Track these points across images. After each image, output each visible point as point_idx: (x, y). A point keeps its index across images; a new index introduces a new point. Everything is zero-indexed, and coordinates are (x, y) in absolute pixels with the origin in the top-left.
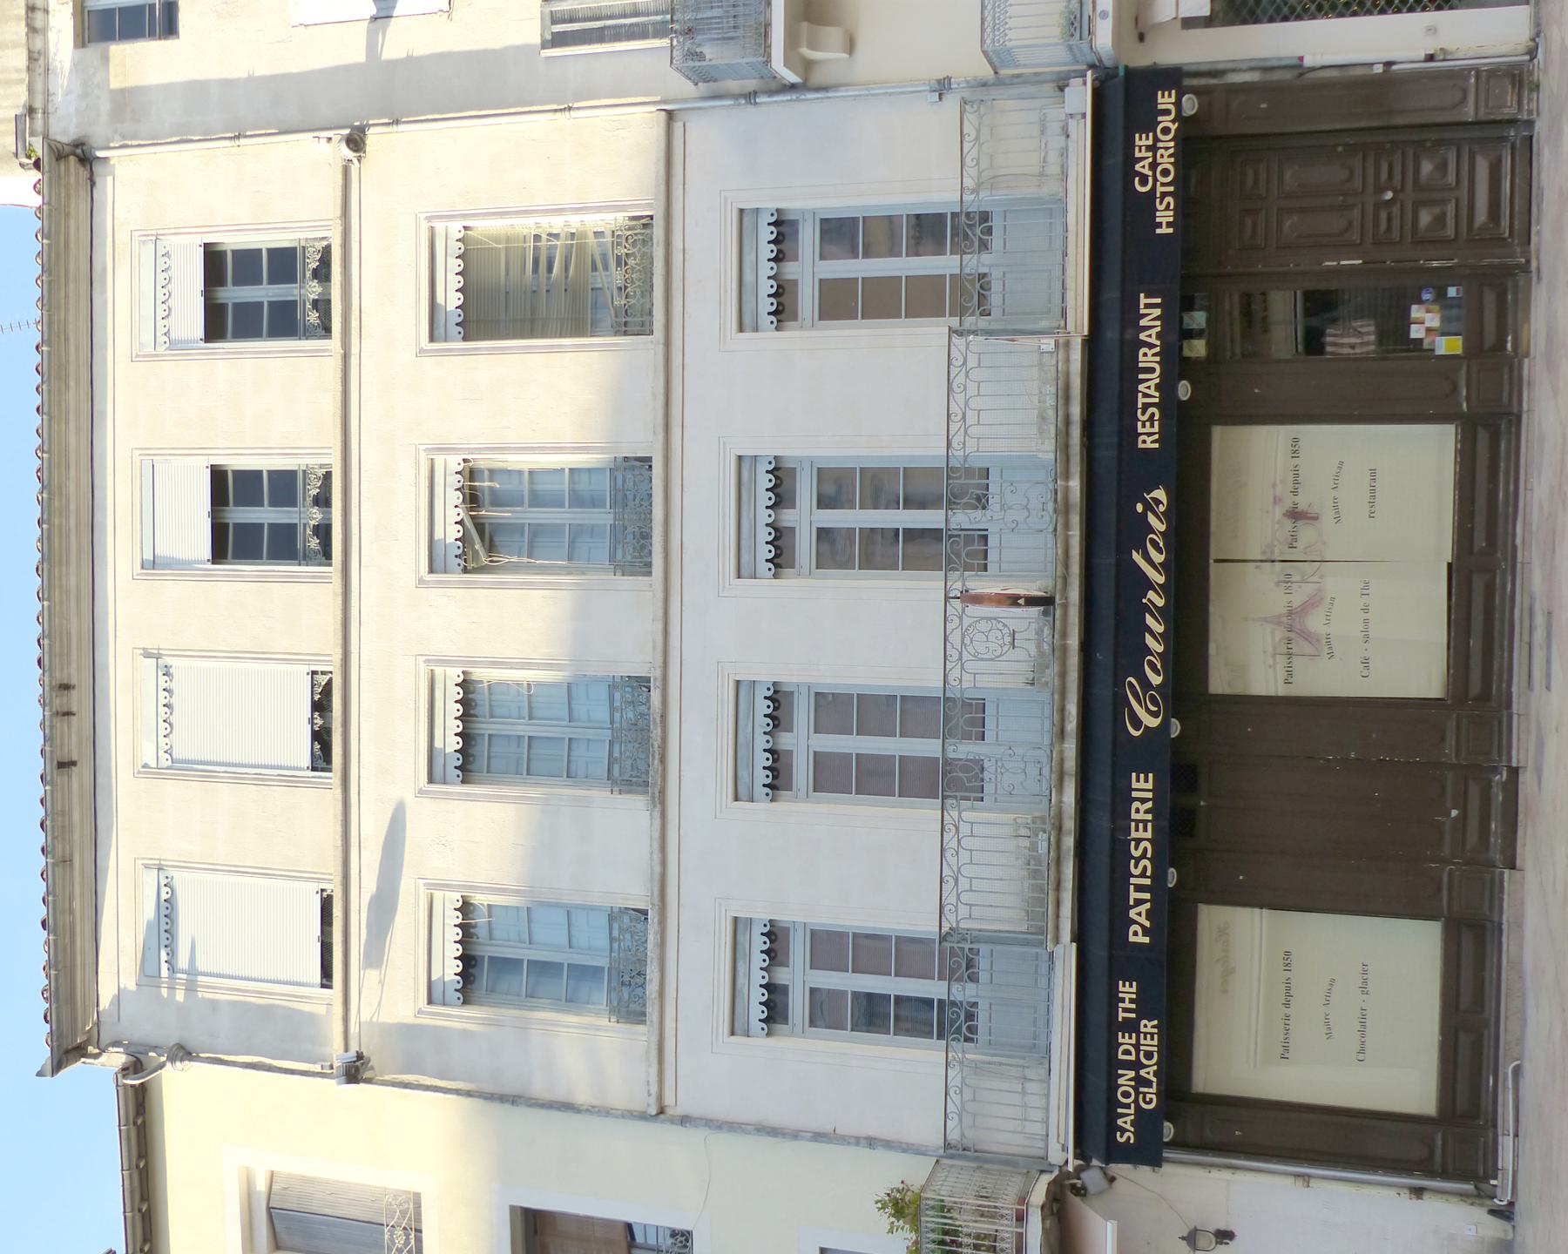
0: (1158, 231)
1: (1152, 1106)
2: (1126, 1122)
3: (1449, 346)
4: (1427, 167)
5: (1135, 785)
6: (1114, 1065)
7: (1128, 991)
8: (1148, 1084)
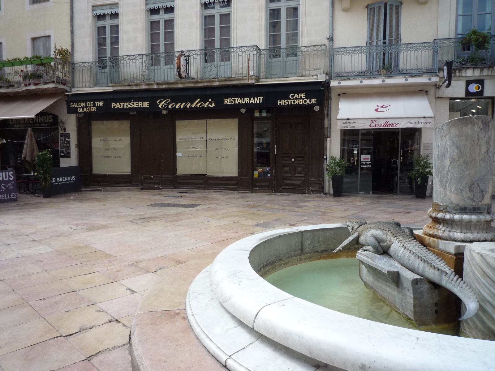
0: (279, 101)
1: (79, 111)
2: (74, 105)
3: (256, 174)
4: (300, 169)
5: (146, 103)
6: (86, 101)
7: (101, 104)
8: (83, 110)
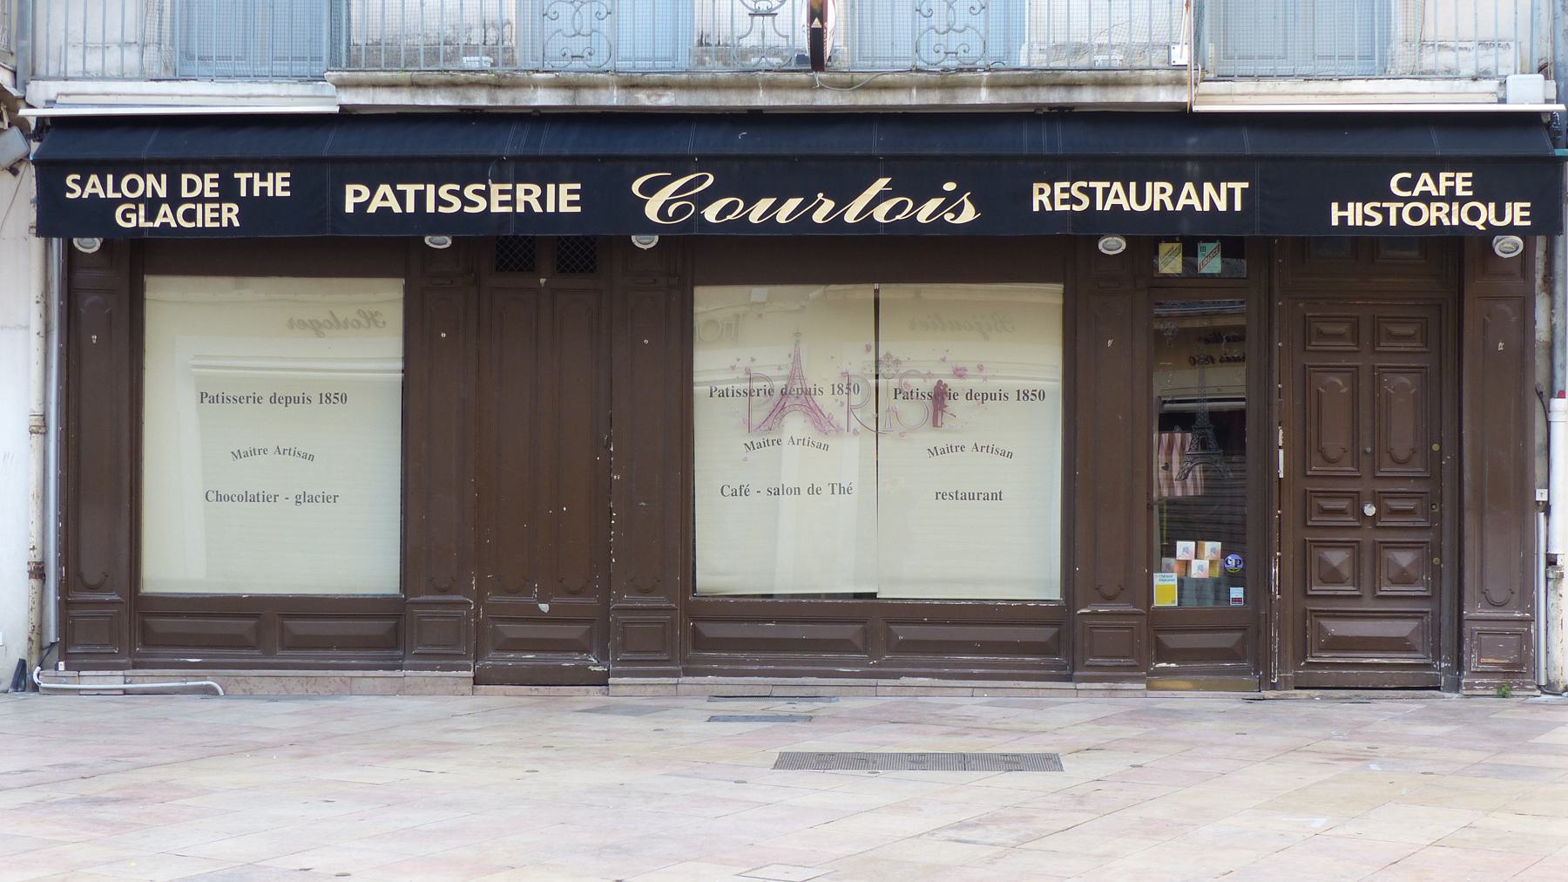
0: (1335, 206)
2: (93, 186)
4: (1405, 559)
5: (564, 188)
6: (172, 168)
7: (277, 185)
8: (151, 216)
